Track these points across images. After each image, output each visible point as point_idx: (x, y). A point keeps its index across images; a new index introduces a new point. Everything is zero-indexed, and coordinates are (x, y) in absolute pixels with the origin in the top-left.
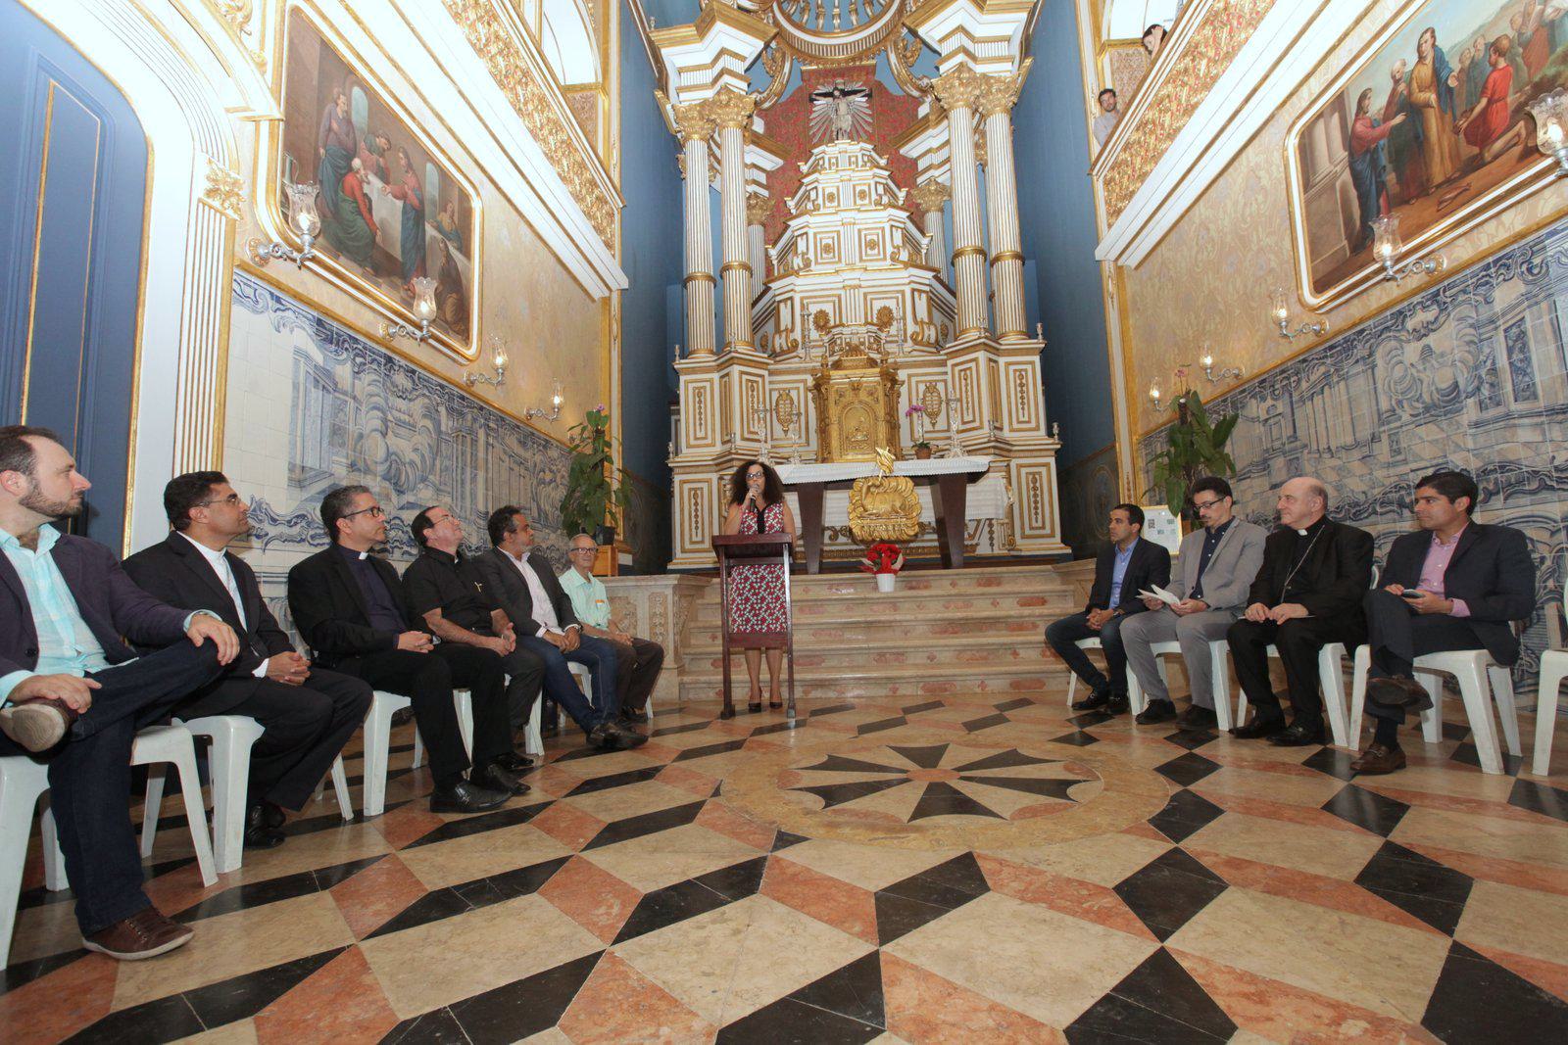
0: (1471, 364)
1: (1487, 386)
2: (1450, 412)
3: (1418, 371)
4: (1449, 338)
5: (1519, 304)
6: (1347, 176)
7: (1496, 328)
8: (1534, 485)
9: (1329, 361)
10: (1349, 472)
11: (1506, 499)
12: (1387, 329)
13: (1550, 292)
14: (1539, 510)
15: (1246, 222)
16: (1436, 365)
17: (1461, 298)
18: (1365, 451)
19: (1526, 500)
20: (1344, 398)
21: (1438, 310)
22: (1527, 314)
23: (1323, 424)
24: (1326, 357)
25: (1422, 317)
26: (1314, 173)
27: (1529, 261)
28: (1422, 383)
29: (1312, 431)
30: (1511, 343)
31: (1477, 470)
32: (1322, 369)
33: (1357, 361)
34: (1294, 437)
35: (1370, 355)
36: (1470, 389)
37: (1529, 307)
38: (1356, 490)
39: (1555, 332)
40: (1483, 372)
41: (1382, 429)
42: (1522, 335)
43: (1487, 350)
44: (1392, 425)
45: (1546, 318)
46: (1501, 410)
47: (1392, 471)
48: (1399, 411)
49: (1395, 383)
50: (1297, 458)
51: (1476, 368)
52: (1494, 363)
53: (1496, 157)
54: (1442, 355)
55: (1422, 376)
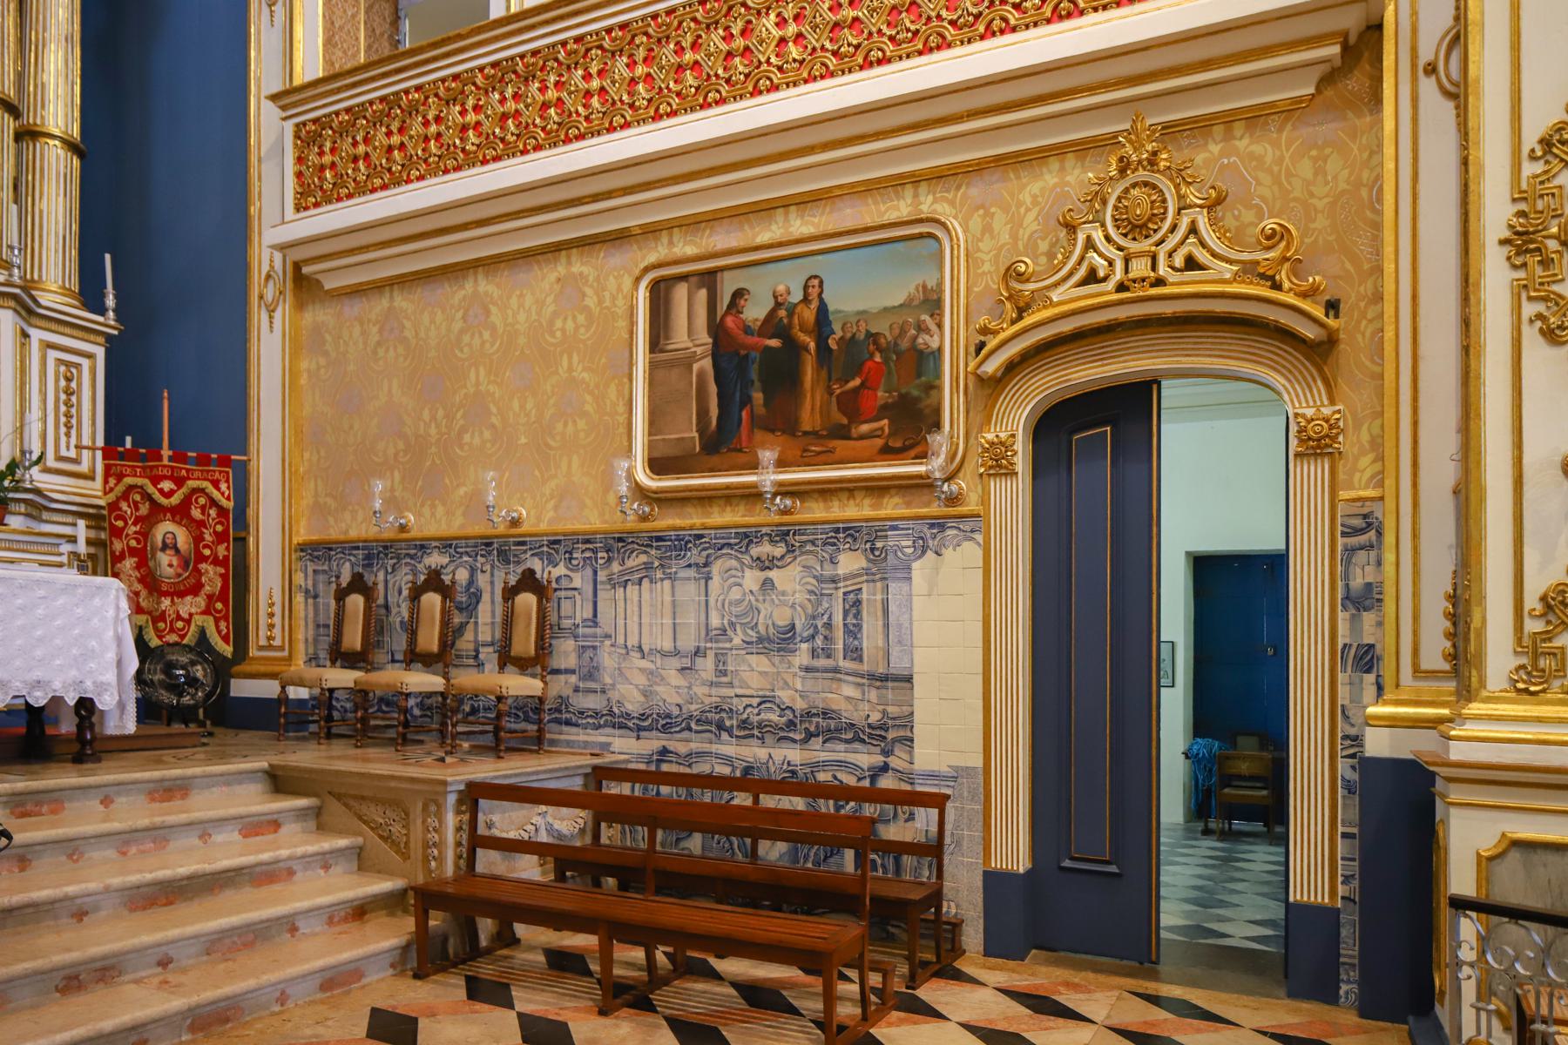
0: (810, 611)
3: (757, 600)
4: (791, 580)
5: (860, 575)
6: (707, 363)
7: (837, 589)
8: (850, 735)
9: (653, 552)
10: (663, 679)
11: (824, 742)
12: (729, 545)
14: (851, 757)
15: (552, 333)
16: (777, 602)
17: (809, 547)
18: (687, 662)
19: (842, 747)
22: (864, 586)
23: (636, 619)
24: (647, 546)
25: (765, 549)
26: (667, 337)
27: (873, 542)
29: (621, 622)
32: (643, 558)
33: (689, 566)
34: (594, 621)
35: (706, 565)
36: (805, 634)
37: (867, 581)
40: (820, 624)
41: (709, 645)
42: (858, 603)
43: (826, 605)
44: (721, 645)
45: (879, 597)
47: (714, 691)
48: (729, 632)
49: (730, 604)
50: (594, 648)
51: (814, 618)
52: (830, 618)
53: (862, 437)
54: (784, 593)
55: (760, 606)
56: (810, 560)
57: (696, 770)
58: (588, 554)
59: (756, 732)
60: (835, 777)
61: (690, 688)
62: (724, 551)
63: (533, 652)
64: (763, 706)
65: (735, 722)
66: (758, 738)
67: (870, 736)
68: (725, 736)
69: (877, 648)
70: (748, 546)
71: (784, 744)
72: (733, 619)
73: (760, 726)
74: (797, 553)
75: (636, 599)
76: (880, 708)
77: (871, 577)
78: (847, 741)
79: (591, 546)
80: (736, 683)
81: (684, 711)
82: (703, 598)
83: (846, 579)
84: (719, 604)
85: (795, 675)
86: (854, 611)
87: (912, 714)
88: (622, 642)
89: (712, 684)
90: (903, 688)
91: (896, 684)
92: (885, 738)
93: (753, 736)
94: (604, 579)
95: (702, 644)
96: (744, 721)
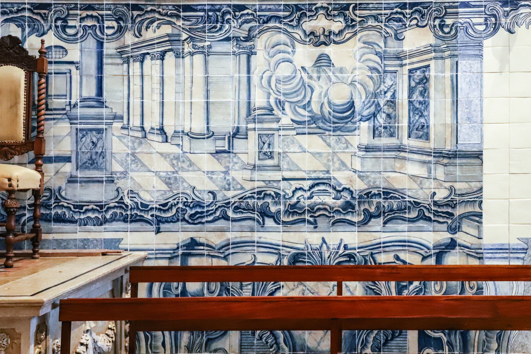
0: (371, 89)
1: (384, 116)
2: (340, 129)
3: (310, 78)
5: (429, 52)
7: (402, 66)
8: (414, 214)
9: (180, 23)
10: (191, 164)
11: (385, 223)
13: (456, 53)
14: (415, 236)
16: (334, 79)
17: (371, 22)
18: (223, 145)
19: (405, 226)
20: (188, 75)
21: (344, 25)
22: (432, 63)
23: (157, 98)
24: (171, 16)
28: (312, 91)
29: (135, 102)
30: (413, 84)
31: (361, 191)
32: (166, 29)
33: (228, 39)
36: (365, 113)
37: (435, 58)
38: (198, 188)
39: (453, 88)
42: (425, 80)
43: (389, 82)
44: (266, 126)
45: (448, 74)
46: (393, 141)
47: (256, 175)
48: (276, 111)
49: (278, 81)
54: (341, 70)
55: (314, 83)
56: (373, 36)
57: (233, 261)
58: (89, 23)
59: (307, 217)
60: (397, 258)
61: (226, 173)
62: (270, 25)
63: (21, 137)
64: (316, 189)
65: (282, 208)
66: (309, 222)
67: (436, 213)
68: (269, 222)
69: (445, 125)
70: (299, 20)
71: (340, 227)
72: (282, 98)
73: (312, 210)
74: (358, 28)
76: (447, 185)
77: (439, 54)
78: (412, 221)
79: (95, 13)
80: (284, 165)
81: (219, 197)
82: (244, 75)
83: (411, 56)
84: (265, 82)
85: (354, 155)
86: (420, 88)
87: (481, 189)
88: (138, 123)
89: (254, 167)
90: (472, 165)
91: (464, 161)
92: (452, 215)
93: (304, 221)
94: (114, 52)
95: (243, 125)
96: (293, 206)
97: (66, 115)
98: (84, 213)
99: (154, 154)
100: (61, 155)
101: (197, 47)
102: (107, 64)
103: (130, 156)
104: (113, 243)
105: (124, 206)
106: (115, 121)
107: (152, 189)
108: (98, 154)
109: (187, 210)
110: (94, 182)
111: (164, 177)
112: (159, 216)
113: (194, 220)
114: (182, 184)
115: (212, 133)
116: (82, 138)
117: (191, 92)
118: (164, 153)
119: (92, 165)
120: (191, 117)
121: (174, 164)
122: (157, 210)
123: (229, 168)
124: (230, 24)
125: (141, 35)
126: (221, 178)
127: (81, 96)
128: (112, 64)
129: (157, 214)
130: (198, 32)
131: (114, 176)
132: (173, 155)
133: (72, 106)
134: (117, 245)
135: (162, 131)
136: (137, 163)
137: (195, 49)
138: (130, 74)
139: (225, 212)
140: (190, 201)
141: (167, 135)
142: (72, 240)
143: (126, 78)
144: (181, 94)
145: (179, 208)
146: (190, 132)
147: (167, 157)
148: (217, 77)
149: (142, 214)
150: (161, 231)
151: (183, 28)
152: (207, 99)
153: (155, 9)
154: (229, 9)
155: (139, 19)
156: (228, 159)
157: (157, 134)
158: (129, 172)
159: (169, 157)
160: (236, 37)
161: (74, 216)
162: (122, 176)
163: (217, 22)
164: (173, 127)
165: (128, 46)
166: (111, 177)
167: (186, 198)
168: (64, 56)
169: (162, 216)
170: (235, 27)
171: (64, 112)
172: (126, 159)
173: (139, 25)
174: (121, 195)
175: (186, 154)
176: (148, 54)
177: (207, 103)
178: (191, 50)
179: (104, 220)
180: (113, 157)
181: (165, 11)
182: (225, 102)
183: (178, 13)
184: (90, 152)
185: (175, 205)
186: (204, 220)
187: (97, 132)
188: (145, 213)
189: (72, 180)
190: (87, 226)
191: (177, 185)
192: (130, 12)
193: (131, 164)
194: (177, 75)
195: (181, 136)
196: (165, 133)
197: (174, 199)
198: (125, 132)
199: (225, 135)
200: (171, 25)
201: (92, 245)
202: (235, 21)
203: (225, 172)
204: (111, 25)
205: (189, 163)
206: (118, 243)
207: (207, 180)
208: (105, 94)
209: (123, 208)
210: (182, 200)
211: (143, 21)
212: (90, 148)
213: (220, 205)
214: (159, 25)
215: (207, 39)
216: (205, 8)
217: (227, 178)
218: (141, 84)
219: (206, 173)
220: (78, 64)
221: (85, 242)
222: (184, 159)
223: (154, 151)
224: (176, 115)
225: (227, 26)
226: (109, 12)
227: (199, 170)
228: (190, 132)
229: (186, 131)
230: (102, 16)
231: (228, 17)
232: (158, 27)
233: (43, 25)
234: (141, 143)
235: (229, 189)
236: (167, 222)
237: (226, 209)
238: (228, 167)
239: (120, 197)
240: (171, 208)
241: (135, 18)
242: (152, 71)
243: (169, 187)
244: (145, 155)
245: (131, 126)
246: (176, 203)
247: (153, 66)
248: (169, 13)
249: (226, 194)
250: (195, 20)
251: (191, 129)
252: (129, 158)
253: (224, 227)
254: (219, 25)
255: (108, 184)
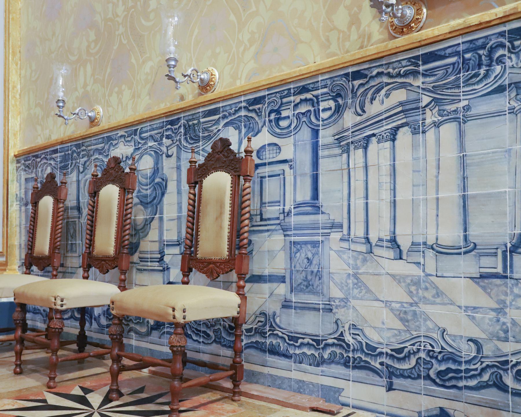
10: (439, 293)
23: (386, 195)
58: (303, 109)
61: (500, 311)
75: (385, 163)
79: (308, 96)
81: (487, 350)
88: (361, 233)
97: (279, 226)
98: (299, 347)
99: (384, 276)
100: (276, 274)
101: (445, 112)
102: (323, 157)
103: (352, 278)
104: (332, 393)
105: (344, 345)
106: (333, 230)
107: (381, 326)
108: (314, 274)
109: (433, 365)
110: (309, 309)
111: (398, 310)
112: (391, 366)
113: (444, 381)
114: (424, 323)
115: (472, 244)
116: (296, 253)
117: (438, 182)
118: (397, 275)
119: (307, 287)
120: (437, 221)
121: (411, 292)
122: (388, 357)
123: (505, 303)
124: (504, 63)
125: (364, 111)
126: (490, 320)
127: (295, 201)
128: (329, 156)
129: (389, 363)
130: (448, 89)
131: (333, 303)
132: (410, 278)
133: (286, 214)
134: (337, 396)
135: (393, 243)
136: (360, 287)
137: (442, 116)
138: (351, 167)
139: (498, 376)
140: (437, 350)
141: (401, 248)
142: (286, 378)
143: (345, 172)
144: (421, 187)
145: (420, 358)
146: (436, 243)
147: (402, 281)
148: (480, 154)
149: (368, 360)
150: (394, 387)
151: (423, 89)
152: (464, 191)
153: (383, 70)
154: (501, 40)
155: (362, 90)
156: (503, 288)
157: (387, 247)
158: (351, 300)
159: (404, 282)
160: (515, 83)
161: (288, 349)
162: (342, 304)
163: (480, 66)
164: (411, 237)
165: (348, 129)
166: (329, 304)
167: (431, 345)
168: (278, 154)
169: (395, 366)
170: (513, 67)
171: (277, 222)
172: (346, 282)
173: (362, 98)
174: (341, 330)
175: (429, 277)
176: (374, 135)
177: (464, 198)
178: (436, 119)
179: (321, 360)
180: (330, 278)
181: (396, 70)
182: (495, 193)
183: (416, 68)
184: (305, 271)
185: (414, 353)
186: (461, 384)
187: (312, 245)
188: (371, 359)
189: (286, 305)
190: (302, 365)
191: (417, 324)
192: (350, 83)
193: (353, 289)
194: (414, 159)
195: (422, 249)
196: (399, 247)
197: (413, 345)
198: (345, 245)
199: (497, 249)
200: (405, 88)
201: (308, 390)
202: (513, 56)
203: (497, 309)
204: (328, 106)
205: (435, 292)
206: (337, 394)
207: (465, 321)
208: (321, 196)
209: (344, 348)
210: (424, 347)
211: (367, 91)
212: (304, 265)
213: (490, 364)
214: (388, 92)
215: (462, 98)
216: (458, 50)
217: (502, 320)
218: (365, 179)
219: (463, 308)
220: (292, 162)
221: (301, 384)
222: (428, 285)
223: (383, 271)
224: (414, 220)
225: (498, 69)
226: (325, 90)
227: (452, 303)
228: (436, 243)
229: (429, 243)
230: (317, 97)
231: (500, 52)
232: (387, 95)
233: (257, 122)
234: (365, 260)
235: (506, 340)
236: (402, 376)
237: (501, 372)
238: (504, 302)
239: (340, 332)
240: (408, 356)
241: (357, 90)
242: (380, 159)
243: (405, 325)
244: (371, 276)
245: (353, 237)
246: (415, 350)
247: (380, 151)
248: (402, 72)
249: (500, 347)
250: (442, 71)
251: (437, 239)
252: (351, 281)
253: (498, 402)
254: (482, 71)
255: (325, 313)
